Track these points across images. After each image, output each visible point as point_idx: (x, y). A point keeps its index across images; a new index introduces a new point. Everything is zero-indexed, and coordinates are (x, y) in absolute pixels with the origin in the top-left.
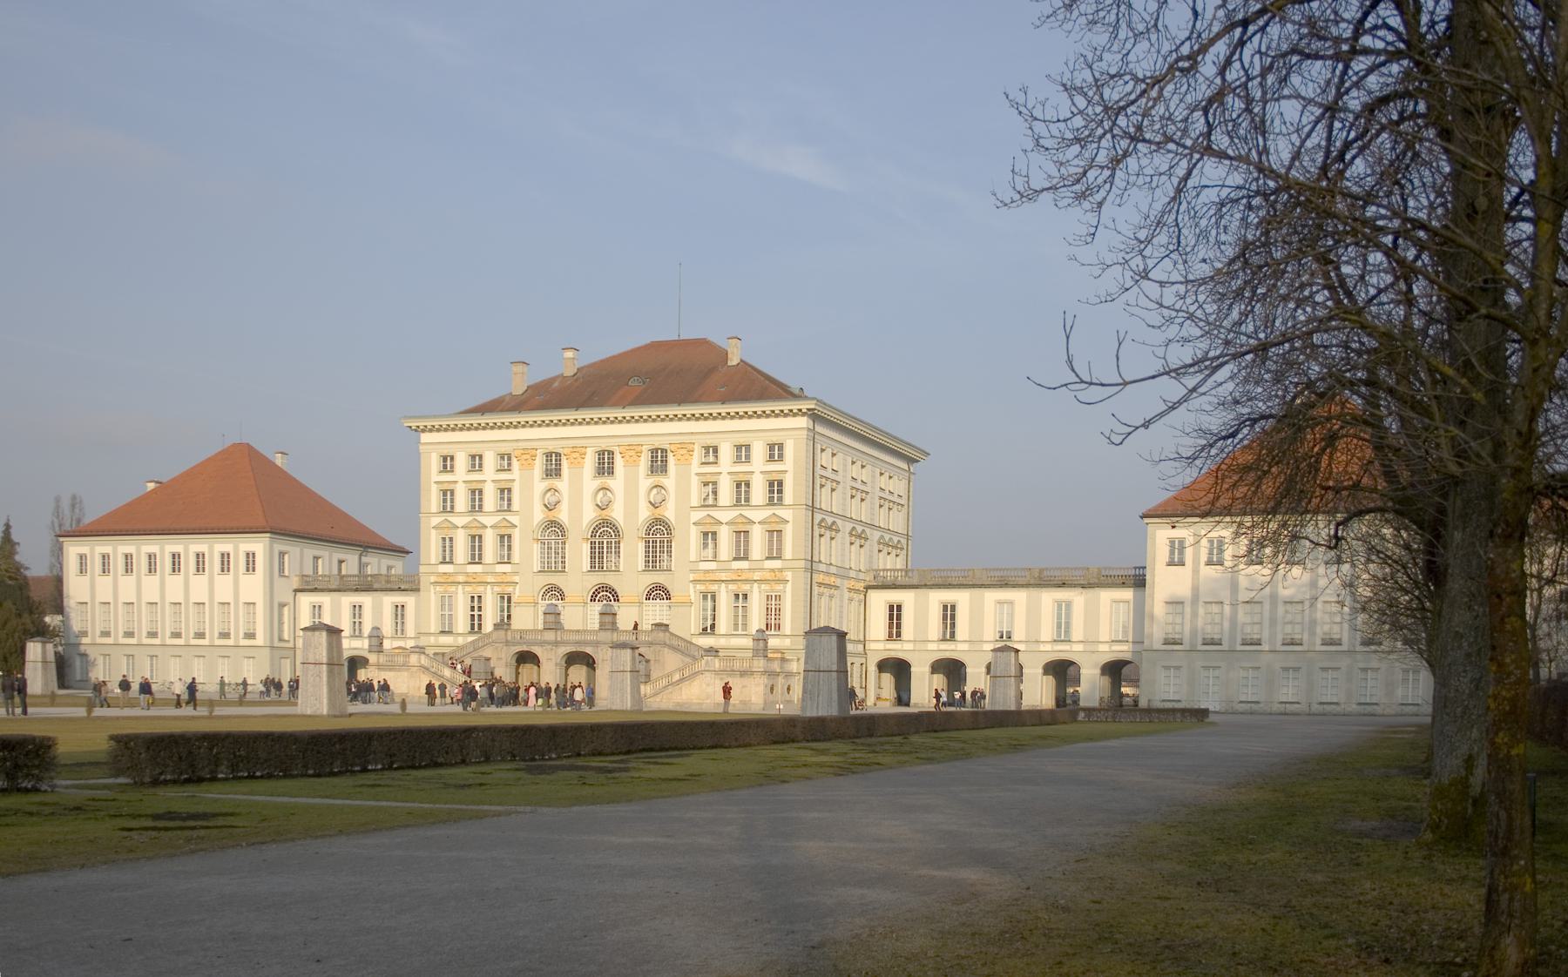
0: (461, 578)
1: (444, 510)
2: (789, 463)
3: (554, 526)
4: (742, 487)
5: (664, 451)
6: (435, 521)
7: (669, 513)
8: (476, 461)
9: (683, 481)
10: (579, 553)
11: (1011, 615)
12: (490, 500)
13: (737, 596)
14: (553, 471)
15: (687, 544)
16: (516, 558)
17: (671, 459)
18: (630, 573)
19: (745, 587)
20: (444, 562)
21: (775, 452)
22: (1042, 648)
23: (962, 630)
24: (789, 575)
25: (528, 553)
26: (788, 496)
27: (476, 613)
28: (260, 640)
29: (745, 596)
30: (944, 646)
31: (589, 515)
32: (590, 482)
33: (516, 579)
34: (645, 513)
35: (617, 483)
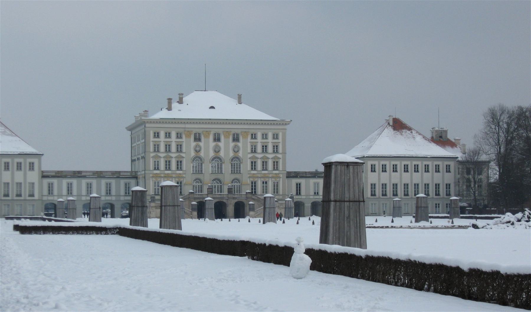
0: (162, 175)
1: (155, 151)
2: (280, 140)
5: (238, 135)
6: (152, 155)
7: (240, 154)
8: (168, 135)
12: (174, 148)
13: (263, 182)
14: (197, 139)
16: (184, 168)
17: (241, 138)
19: (267, 179)
20: (155, 169)
24: (281, 176)
26: (280, 150)
28: (36, 197)
29: (266, 182)
31: (212, 154)
32: (212, 144)
33: (184, 176)
34: (231, 154)
35: (221, 144)
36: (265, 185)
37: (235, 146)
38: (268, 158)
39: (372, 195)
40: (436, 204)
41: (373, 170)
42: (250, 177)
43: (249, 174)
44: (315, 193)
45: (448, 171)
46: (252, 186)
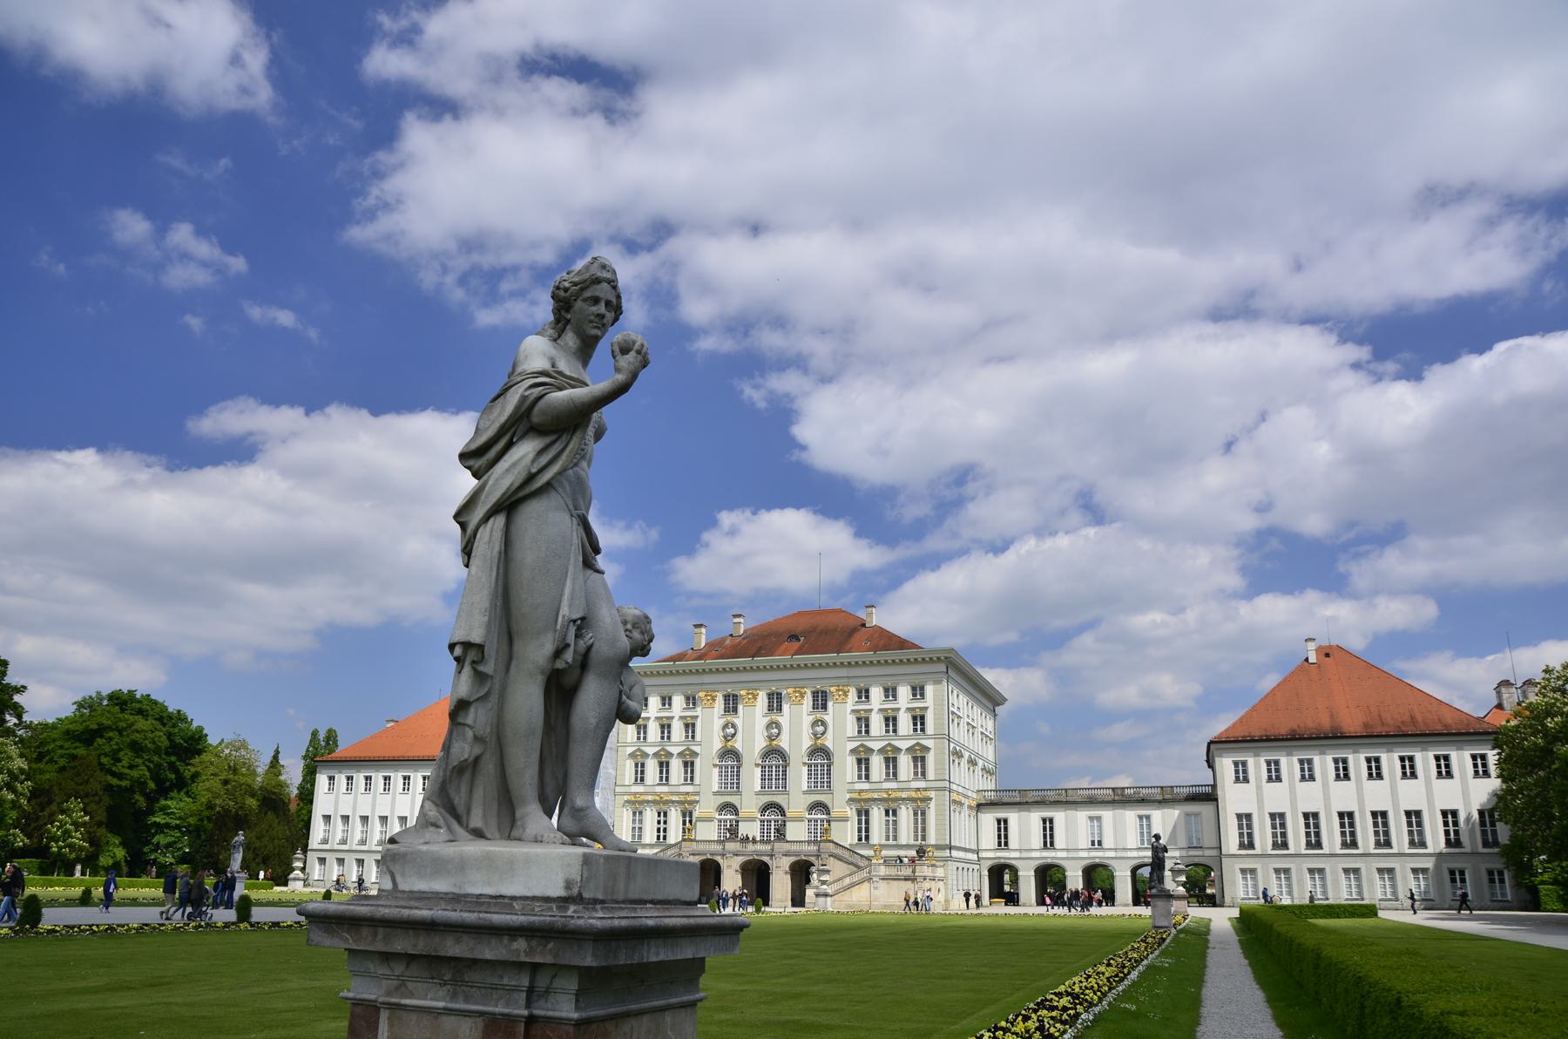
0: (650, 798)
3: (729, 753)
4: (891, 721)
6: (630, 750)
7: (828, 742)
9: (842, 713)
10: (752, 778)
11: (1100, 827)
13: (887, 813)
15: (845, 768)
16: (697, 780)
18: (798, 791)
21: (918, 692)
22: (1130, 854)
23: (1060, 841)
24: (932, 794)
25: (709, 777)
27: (662, 826)
29: (895, 813)
30: (1046, 854)
31: (760, 743)
34: (807, 743)
35: (784, 719)
36: (891, 818)
37: (815, 723)
38: (898, 750)
39: (1242, 846)
40: (1452, 872)
41: (1242, 776)
42: (851, 800)
43: (850, 791)
44: (1093, 843)
45: (1481, 770)
46: (860, 822)
